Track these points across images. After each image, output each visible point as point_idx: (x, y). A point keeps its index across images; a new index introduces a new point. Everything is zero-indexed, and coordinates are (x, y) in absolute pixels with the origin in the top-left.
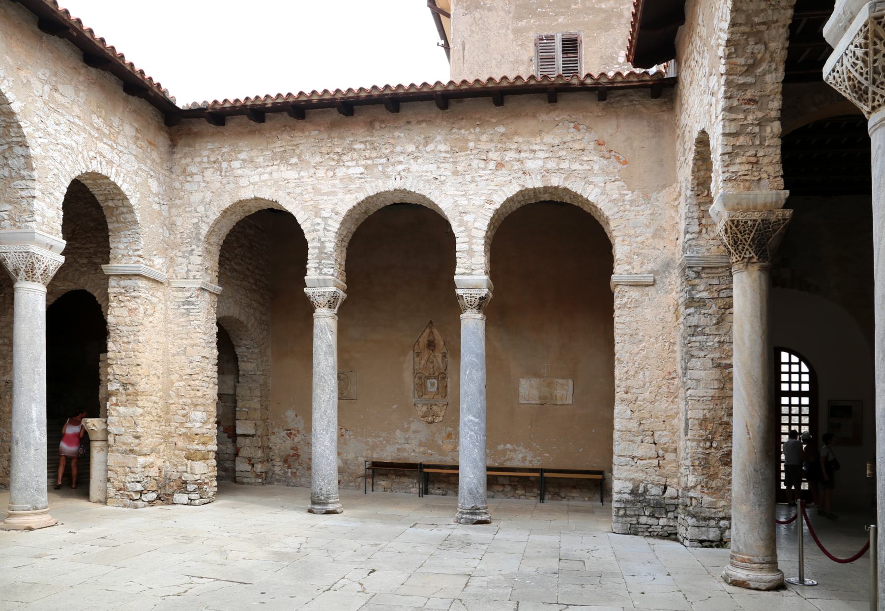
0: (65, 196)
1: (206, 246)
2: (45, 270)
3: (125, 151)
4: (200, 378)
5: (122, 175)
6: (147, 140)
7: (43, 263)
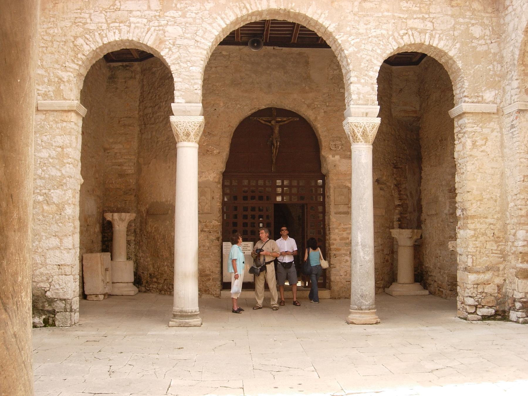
0: (379, 73)
2: (364, 132)
3: (439, 15)
4: (522, 197)
5: (437, 36)
7: (361, 127)
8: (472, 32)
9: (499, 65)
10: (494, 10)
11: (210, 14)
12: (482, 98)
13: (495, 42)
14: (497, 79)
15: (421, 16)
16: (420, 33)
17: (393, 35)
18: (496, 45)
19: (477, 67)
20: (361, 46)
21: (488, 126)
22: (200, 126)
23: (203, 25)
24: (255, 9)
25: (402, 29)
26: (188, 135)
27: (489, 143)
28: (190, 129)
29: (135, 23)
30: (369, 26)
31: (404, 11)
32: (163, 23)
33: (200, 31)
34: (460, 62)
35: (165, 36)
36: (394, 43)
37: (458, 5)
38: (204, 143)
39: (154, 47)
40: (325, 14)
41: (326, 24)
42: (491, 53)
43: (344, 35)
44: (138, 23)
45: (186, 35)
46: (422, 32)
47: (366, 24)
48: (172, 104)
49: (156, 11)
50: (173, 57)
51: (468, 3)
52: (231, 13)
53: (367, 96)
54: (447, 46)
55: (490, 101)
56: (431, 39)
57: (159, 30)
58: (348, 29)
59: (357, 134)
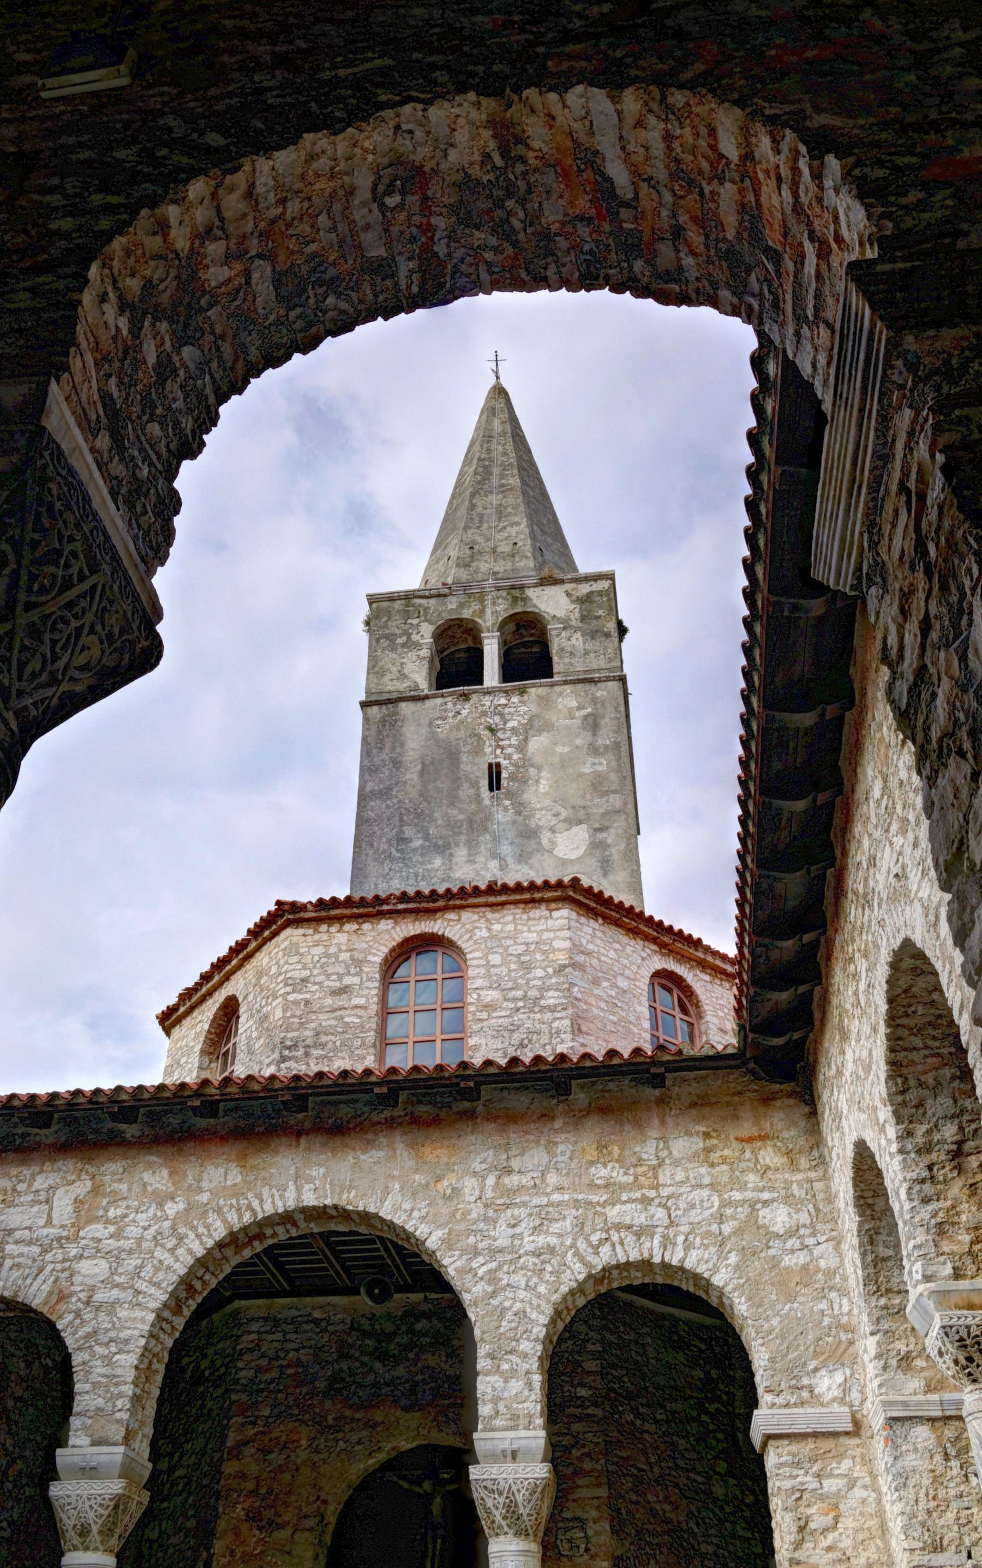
1: (883, 1301)
5: (681, 1239)
6: (737, 1139)
7: (500, 1494)
8: (766, 1221)
9: (845, 1301)
10: (814, 1163)
11: (173, 1228)
12: (811, 1392)
13: (827, 1241)
14: (843, 1337)
15: (638, 1195)
16: (638, 1235)
17: (573, 1246)
18: (831, 1250)
19: (787, 1307)
20: (500, 1280)
21: (838, 1472)
22: (116, 1507)
23: (156, 1254)
24: (269, 1209)
25: (595, 1231)
26: (84, 1532)
27: (847, 1523)
28: (91, 1514)
29: (13, 1258)
30: (518, 1230)
31: (599, 1187)
32: (73, 1252)
33: (147, 1269)
34: (743, 1299)
35: (72, 1284)
36: (578, 1266)
37: (724, 1160)
38: (255, 1549)
39: (45, 1310)
40: (419, 1210)
41: (421, 1231)
42: (818, 1269)
43: (461, 1256)
44: (21, 1255)
45: (118, 1279)
46: (642, 1232)
47: (514, 1226)
48: (59, 1452)
49: (63, 1227)
50: (81, 1333)
51: (748, 1155)
52: (218, 1223)
53: (515, 1406)
54: (707, 1261)
55: (834, 1399)
56: (665, 1249)
57: (63, 1271)
58: (472, 1240)
59: (494, 1511)
